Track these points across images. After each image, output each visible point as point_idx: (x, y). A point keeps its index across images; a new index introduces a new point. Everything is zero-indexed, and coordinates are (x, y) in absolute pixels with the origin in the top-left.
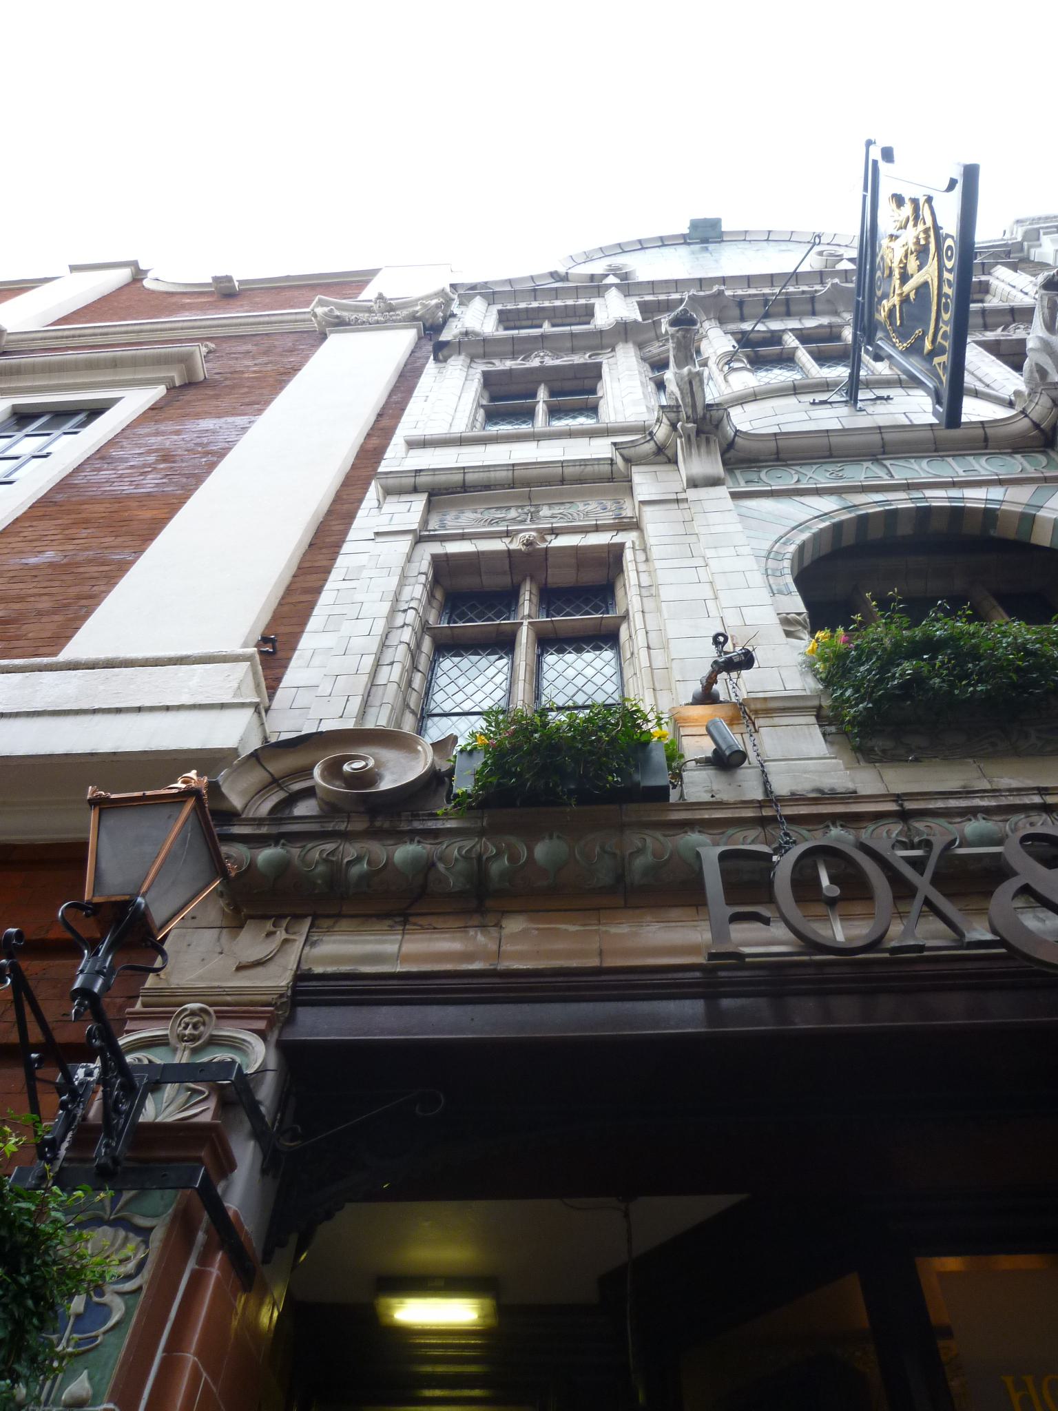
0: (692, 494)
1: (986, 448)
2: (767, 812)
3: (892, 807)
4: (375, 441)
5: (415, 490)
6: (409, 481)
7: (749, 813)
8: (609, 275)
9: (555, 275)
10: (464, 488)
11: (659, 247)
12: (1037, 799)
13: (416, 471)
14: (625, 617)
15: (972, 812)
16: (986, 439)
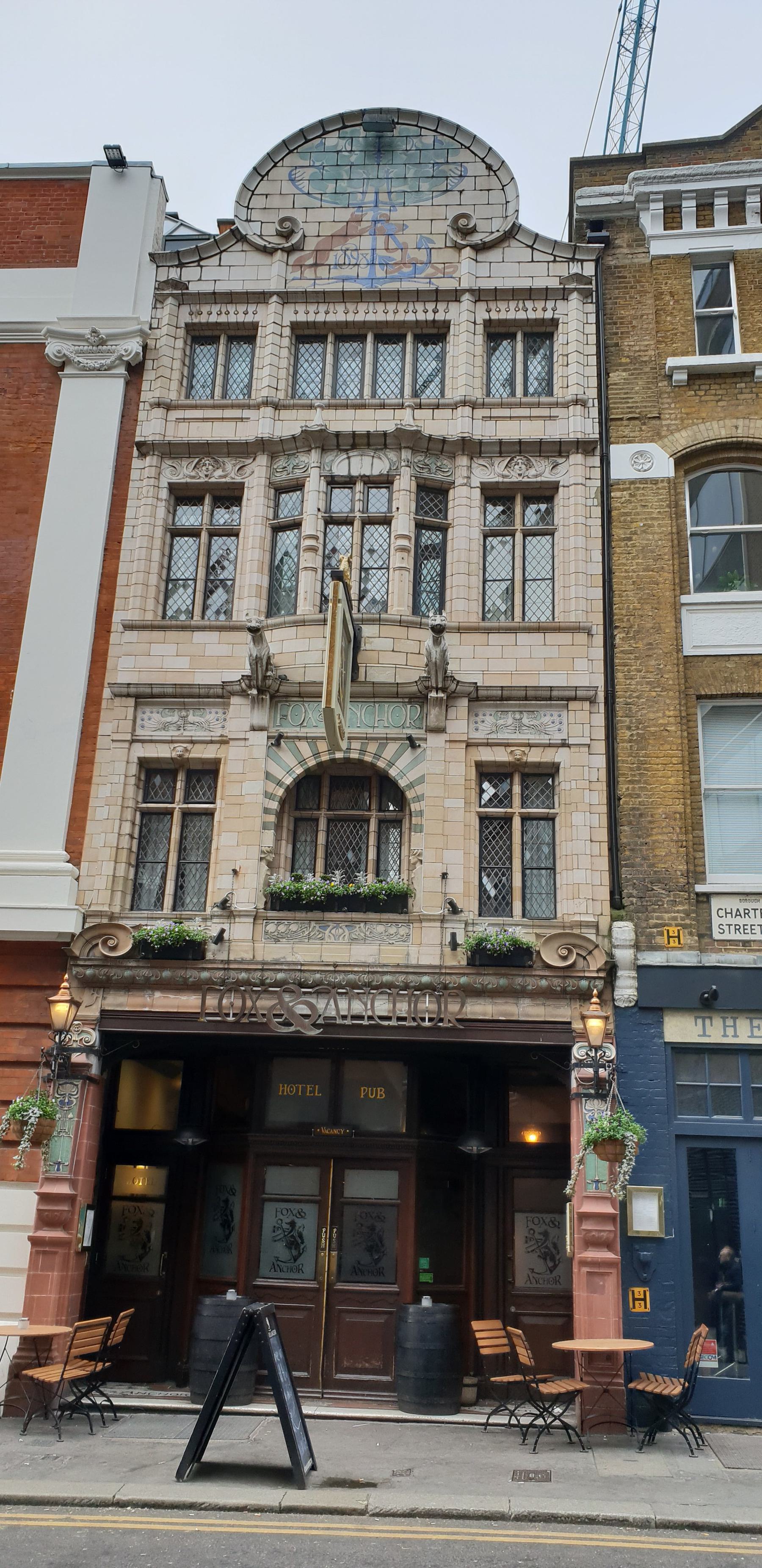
0: (251, 735)
1: (397, 697)
2: (226, 966)
3: (260, 967)
4: (105, 598)
5: (128, 696)
6: (124, 690)
7: (221, 966)
8: (276, 250)
9: (236, 233)
10: (152, 696)
11: (338, 129)
12: (299, 967)
13: (129, 684)
14: (215, 809)
15: (281, 970)
16: (397, 693)
